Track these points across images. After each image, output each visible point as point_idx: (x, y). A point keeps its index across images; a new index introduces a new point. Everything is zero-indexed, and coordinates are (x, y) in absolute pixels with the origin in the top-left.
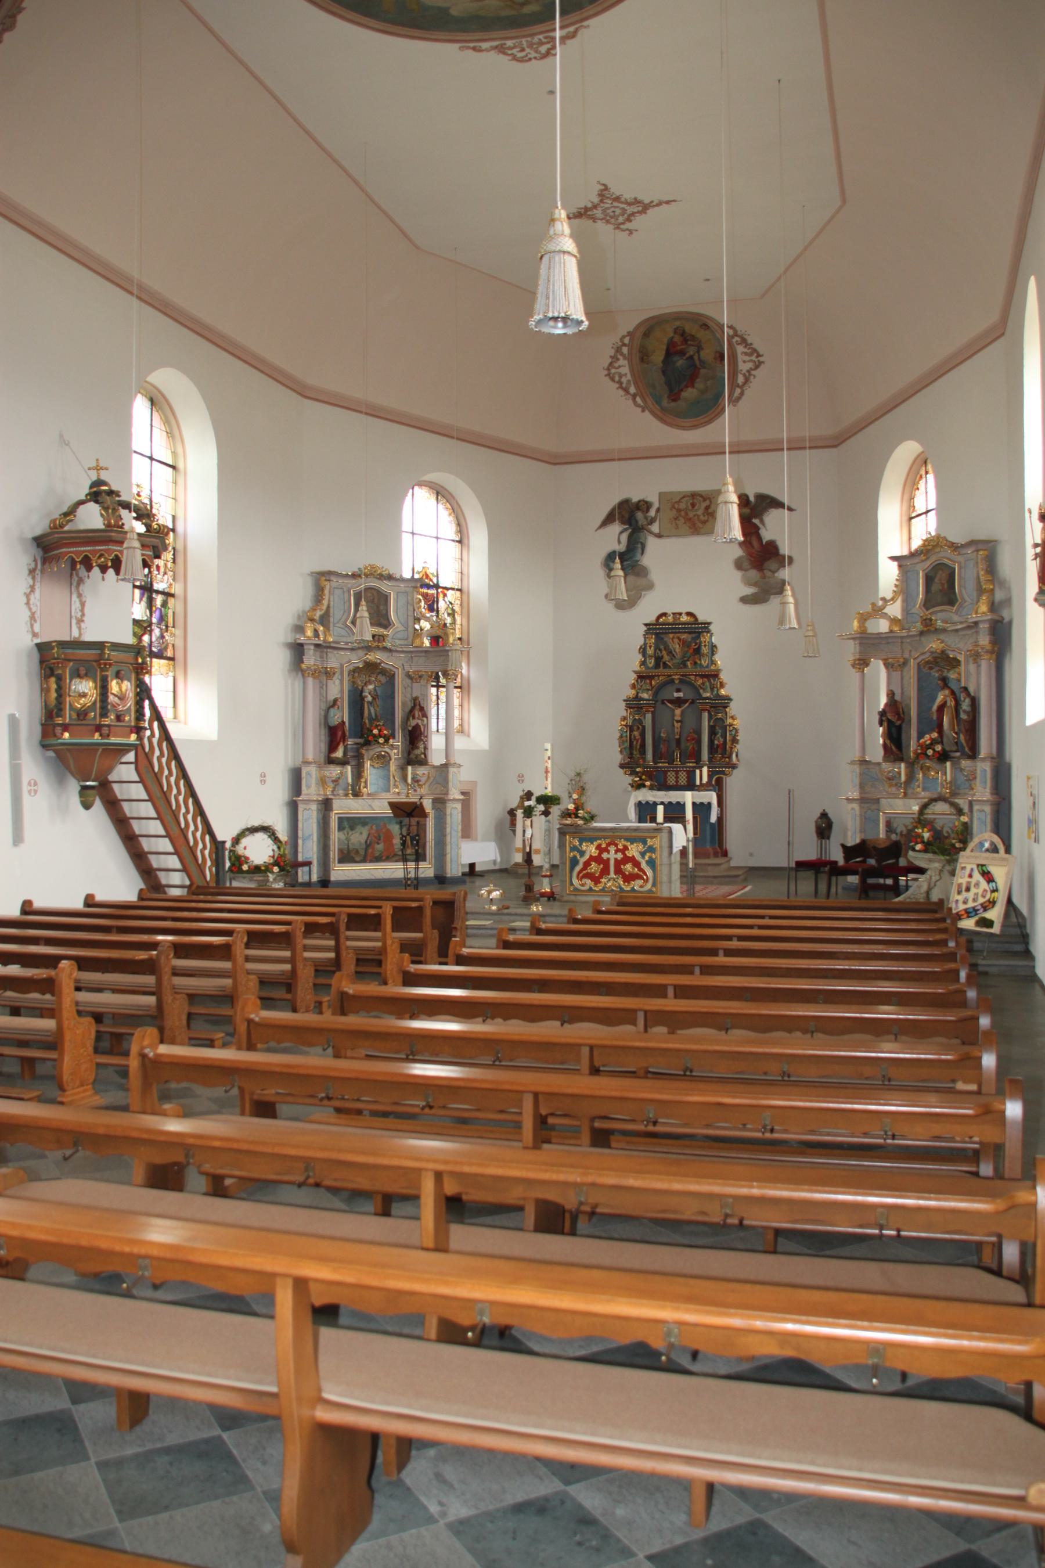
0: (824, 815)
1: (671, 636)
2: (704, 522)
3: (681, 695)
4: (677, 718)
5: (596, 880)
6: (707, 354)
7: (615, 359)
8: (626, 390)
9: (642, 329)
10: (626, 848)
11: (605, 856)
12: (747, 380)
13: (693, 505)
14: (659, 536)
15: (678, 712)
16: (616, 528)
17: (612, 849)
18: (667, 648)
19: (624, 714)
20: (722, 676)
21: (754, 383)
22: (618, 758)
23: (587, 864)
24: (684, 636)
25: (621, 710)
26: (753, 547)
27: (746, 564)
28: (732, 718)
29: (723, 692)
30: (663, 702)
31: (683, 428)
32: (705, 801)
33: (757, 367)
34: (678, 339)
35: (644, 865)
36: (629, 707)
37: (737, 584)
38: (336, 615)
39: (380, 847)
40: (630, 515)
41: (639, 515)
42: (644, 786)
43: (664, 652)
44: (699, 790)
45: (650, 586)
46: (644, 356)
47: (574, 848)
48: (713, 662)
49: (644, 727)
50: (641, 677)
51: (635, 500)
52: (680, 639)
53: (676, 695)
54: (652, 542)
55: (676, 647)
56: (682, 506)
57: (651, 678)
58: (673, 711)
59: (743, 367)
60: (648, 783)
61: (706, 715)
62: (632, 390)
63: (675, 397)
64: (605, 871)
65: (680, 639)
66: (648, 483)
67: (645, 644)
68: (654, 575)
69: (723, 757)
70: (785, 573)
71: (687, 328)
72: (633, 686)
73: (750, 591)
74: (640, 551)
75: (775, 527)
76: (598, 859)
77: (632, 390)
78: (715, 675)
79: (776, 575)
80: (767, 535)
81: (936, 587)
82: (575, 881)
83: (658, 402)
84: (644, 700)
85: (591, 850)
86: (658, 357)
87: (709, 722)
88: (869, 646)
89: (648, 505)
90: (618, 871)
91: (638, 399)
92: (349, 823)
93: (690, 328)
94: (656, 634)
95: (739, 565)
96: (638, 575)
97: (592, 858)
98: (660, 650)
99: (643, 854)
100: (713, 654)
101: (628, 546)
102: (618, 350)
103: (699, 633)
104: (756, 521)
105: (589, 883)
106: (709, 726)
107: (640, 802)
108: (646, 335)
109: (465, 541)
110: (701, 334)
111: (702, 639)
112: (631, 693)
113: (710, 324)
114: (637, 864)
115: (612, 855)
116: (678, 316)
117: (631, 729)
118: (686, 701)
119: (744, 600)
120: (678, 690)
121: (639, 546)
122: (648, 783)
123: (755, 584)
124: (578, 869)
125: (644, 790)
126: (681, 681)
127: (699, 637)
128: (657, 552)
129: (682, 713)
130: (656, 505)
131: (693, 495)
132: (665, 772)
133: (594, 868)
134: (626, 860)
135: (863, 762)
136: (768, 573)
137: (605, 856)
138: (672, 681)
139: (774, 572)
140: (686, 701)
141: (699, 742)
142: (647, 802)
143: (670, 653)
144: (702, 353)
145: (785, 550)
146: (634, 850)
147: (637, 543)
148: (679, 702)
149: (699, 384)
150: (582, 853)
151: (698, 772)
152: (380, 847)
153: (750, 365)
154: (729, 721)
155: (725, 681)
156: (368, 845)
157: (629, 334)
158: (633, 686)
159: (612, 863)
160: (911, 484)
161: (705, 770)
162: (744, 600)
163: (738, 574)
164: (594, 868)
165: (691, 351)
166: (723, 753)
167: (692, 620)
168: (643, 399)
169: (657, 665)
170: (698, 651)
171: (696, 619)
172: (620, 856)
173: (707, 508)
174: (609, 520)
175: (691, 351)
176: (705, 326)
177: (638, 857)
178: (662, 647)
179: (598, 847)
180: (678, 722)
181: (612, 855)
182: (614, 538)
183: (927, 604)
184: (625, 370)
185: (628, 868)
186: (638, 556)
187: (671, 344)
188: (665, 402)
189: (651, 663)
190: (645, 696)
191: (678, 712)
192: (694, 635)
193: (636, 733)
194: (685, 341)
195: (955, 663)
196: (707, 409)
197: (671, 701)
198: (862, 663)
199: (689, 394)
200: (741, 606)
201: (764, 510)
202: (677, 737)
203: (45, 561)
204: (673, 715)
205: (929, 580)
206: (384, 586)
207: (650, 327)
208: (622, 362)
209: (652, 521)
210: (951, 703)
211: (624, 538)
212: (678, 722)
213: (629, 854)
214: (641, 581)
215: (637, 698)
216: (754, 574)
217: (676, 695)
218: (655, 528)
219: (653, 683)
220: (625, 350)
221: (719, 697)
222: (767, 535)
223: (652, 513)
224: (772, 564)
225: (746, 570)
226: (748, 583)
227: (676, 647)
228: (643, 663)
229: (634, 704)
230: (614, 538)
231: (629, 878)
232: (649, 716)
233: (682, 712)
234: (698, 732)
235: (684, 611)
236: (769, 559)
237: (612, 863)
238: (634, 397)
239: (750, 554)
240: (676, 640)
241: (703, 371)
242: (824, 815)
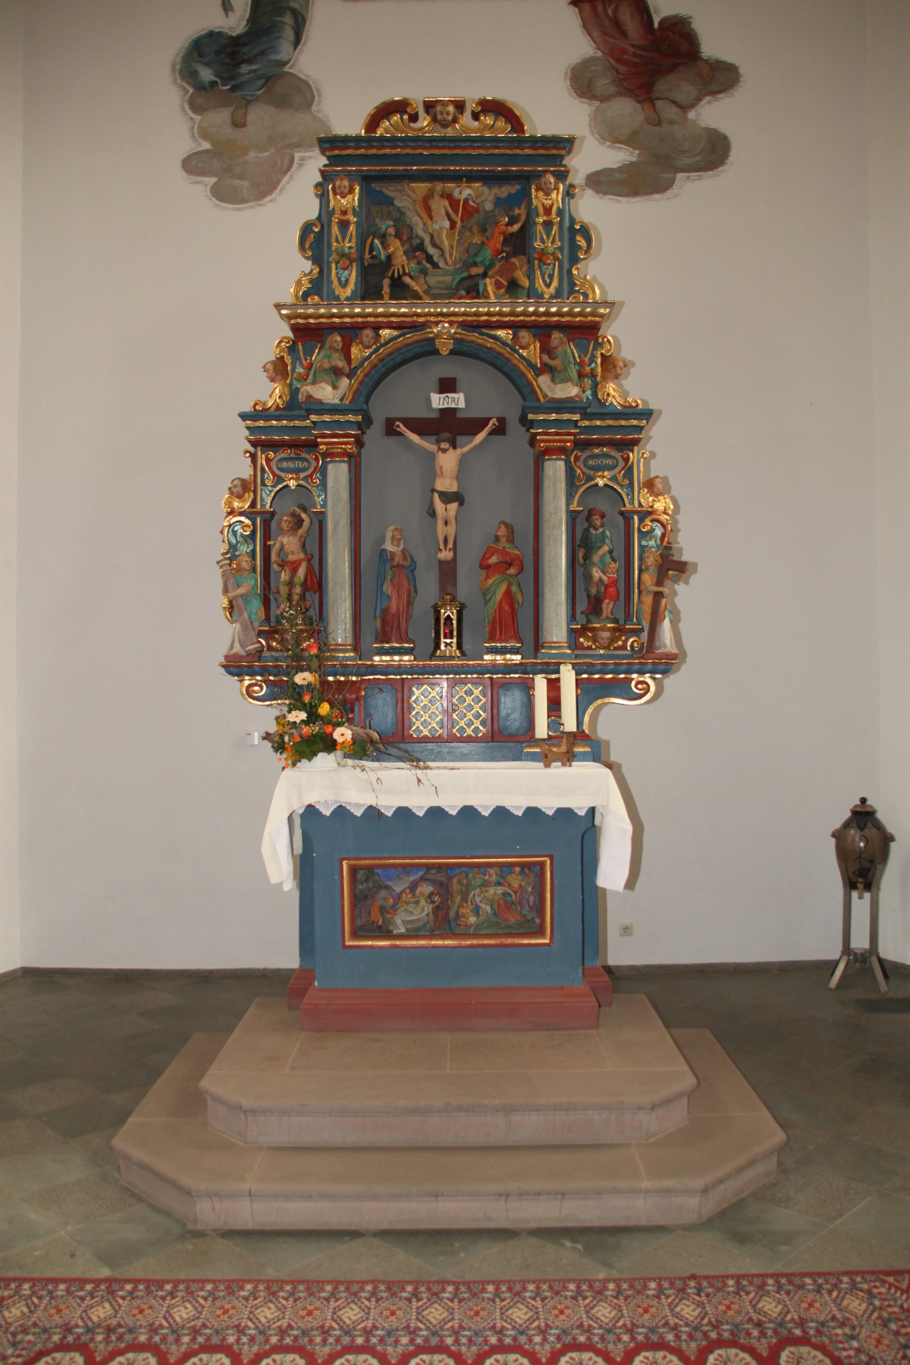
0: (863, 816)
1: (421, 188)
3: (457, 400)
4: (447, 484)
18: (403, 231)
19: (246, 471)
20: (610, 332)
22: (224, 636)
24: (464, 192)
26: (624, 34)
27: (603, 84)
28: (650, 484)
30: (390, 430)
32: (580, 805)
36: (261, 443)
42: (330, 745)
43: (396, 247)
44: (547, 759)
48: (570, 287)
49: (320, 521)
50: (306, 334)
52: (454, 204)
53: (438, 401)
55: (438, 227)
57: (351, 332)
58: (432, 457)
60: (343, 734)
61: (555, 469)
65: (454, 204)
67: (326, 214)
69: (619, 631)
70: (712, 114)
72: (279, 370)
74: (289, 34)
78: (586, 331)
79: (692, 115)
84: (323, 408)
87: (568, 503)
94: (367, 180)
96: (282, 102)
98: (383, 238)
100: (574, 260)
101: (253, 19)
103: (526, 179)
106: (572, 517)
107: (311, 810)
111: (538, 199)
112: (272, 394)
117: (266, 523)
118: (474, 426)
120: (447, 386)
121: (288, 19)
122: (343, 734)
123: (631, 141)
125: (324, 761)
126: (460, 351)
127: (525, 195)
129: (459, 476)
132: (401, 692)
136: (668, 111)
138: (428, 350)
139: (685, 108)
140: (474, 426)
142: (341, 811)
143: (416, 249)
147: (280, 11)
148: (449, 427)
151: (541, 684)
154: (645, 499)
155: (626, 353)
158: (279, 370)
161: (568, 677)
166: (624, 614)
167: (502, 129)
169: (369, 291)
170: (519, 243)
171: (515, 122)
178: (387, 226)
180: (447, 498)
186: (285, 49)
190: (326, 393)
191: (448, 460)
192: (504, 191)
197: (421, 426)
202: (446, 555)
204: (431, 471)
212: (447, 498)
215: (295, 405)
216: (626, 110)
217: (438, 401)
219: (355, 351)
221: (594, 408)
224: (678, 86)
225: (604, 99)
227: (438, 227)
228: (318, 286)
229: (282, 436)
232: (338, 473)
233: (463, 462)
235: (472, 94)
236: (672, 69)
239: (615, 55)
240: (440, 206)
242: (863, 816)
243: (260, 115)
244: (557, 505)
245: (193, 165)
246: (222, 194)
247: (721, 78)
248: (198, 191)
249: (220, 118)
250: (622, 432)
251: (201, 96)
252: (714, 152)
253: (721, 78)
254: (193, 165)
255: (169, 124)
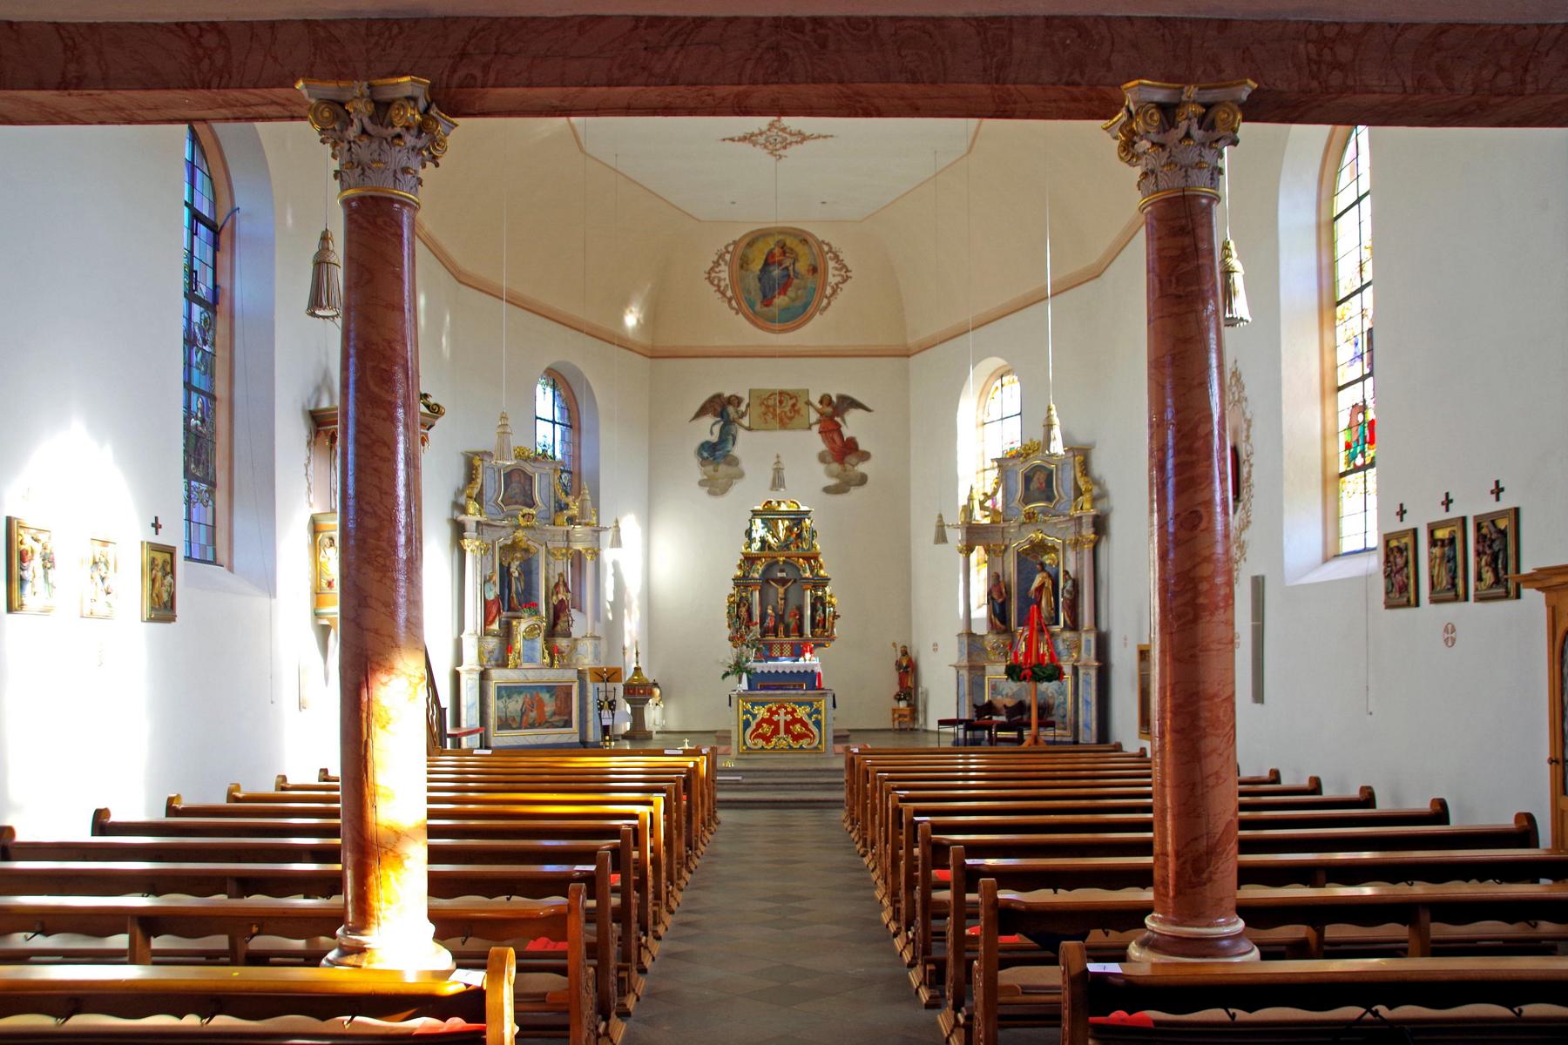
2: (791, 418)
5: (768, 740)
6: (802, 266)
7: (717, 264)
8: (723, 294)
9: (747, 240)
10: (795, 710)
11: (775, 718)
12: (834, 292)
13: (781, 402)
14: (749, 429)
15: (781, 590)
16: (709, 420)
17: (782, 711)
21: (841, 295)
22: (728, 632)
23: (759, 725)
25: (729, 588)
27: (829, 458)
29: (822, 572)
31: (773, 331)
33: (844, 281)
34: (777, 251)
35: (812, 727)
36: (737, 585)
37: (822, 476)
38: (489, 494)
39: (533, 714)
40: (720, 407)
41: (731, 409)
45: (741, 475)
46: (744, 263)
47: (746, 712)
48: (813, 546)
51: (727, 394)
54: (742, 435)
56: (771, 402)
59: (832, 280)
62: (729, 293)
63: (767, 302)
64: (776, 732)
66: (737, 381)
68: (745, 465)
70: (862, 468)
71: (788, 242)
72: (740, 567)
73: (832, 482)
75: (853, 425)
76: (769, 721)
77: (729, 293)
78: (816, 559)
80: (847, 432)
81: (1034, 485)
82: (749, 742)
83: (752, 306)
85: (762, 712)
86: (757, 266)
88: (974, 536)
89: (739, 401)
90: (787, 731)
91: (734, 303)
92: (506, 691)
93: (790, 242)
95: (822, 458)
96: (729, 464)
97: (763, 720)
99: (810, 716)
102: (721, 256)
104: (838, 419)
105: (761, 743)
108: (750, 245)
109: (575, 425)
110: (800, 249)
113: (810, 240)
114: (804, 724)
115: (782, 718)
116: (783, 231)
119: (827, 490)
124: (749, 731)
128: (746, 445)
130: (746, 401)
131: (781, 393)
133: (766, 729)
134: (795, 721)
135: (970, 635)
137: (775, 718)
141: (802, 616)
144: (798, 265)
145: (862, 446)
146: (801, 712)
148: (783, 582)
149: (791, 292)
150: (754, 716)
152: (533, 714)
153: (839, 279)
156: (523, 714)
157: (735, 243)
158: (740, 567)
159: (782, 724)
160: (984, 392)
162: (827, 490)
163: (821, 467)
164: (766, 729)
165: (787, 263)
166: (822, 626)
168: (738, 303)
169: (762, 549)
170: (799, 536)
172: (789, 717)
173: (794, 405)
174: (702, 412)
175: (787, 263)
176: (805, 241)
177: (806, 719)
179: (769, 710)
181: (782, 718)
182: (708, 429)
183: (1027, 500)
184: (725, 275)
185: (798, 728)
187: (771, 254)
188: (758, 307)
189: (756, 545)
193: (743, 610)
194: (784, 253)
195: (1054, 549)
196: (795, 317)
198: (969, 549)
199: (780, 301)
200: (824, 495)
201: (846, 410)
203: (317, 433)
205: (1028, 479)
206: (528, 468)
207: (754, 239)
208: (723, 267)
209: (743, 415)
210: (1049, 584)
211: (717, 429)
213: (798, 716)
214: (732, 470)
216: (836, 467)
218: (745, 421)
220: (728, 257)
222: (847, 432)
223: (743, 408)
224: (851, 459)
226: (831, 474)
229: (742, 583)
230: (708, 429)
231: (797, 737)
232: (757, 594)
234: (800, 609)
237: (782, 724)
238: (730, 300)
239: (832, 449)
241: (796, 281)
243: (723, 468)
244: (808, 601)
245: (702, 483)
246: (711, 493)
247: (865, 456)
248: (703, 492)
249: (710, 468)
250: (822, 582)
251: (704, 462)
252: (863, 480)
253: (865, 456)
254: (702, 483)
255: (694, 470)
